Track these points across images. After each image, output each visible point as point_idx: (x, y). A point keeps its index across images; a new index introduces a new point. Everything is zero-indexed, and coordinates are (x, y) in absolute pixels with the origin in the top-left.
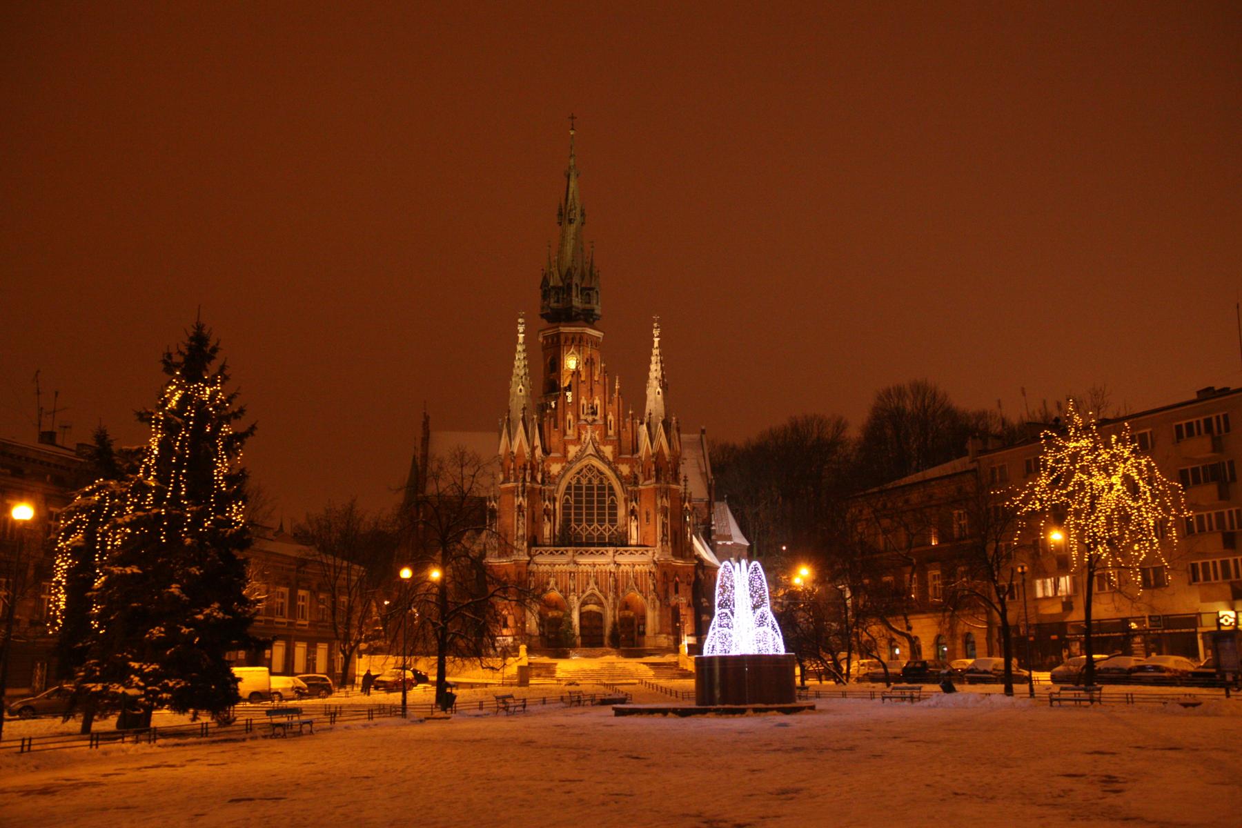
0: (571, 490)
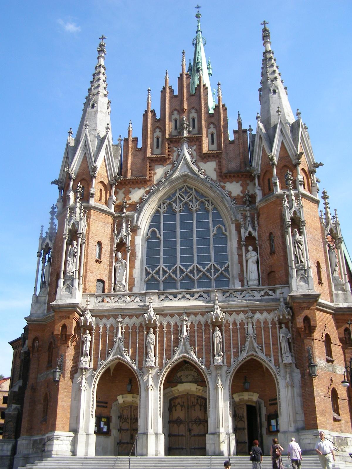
0: (159, 221)
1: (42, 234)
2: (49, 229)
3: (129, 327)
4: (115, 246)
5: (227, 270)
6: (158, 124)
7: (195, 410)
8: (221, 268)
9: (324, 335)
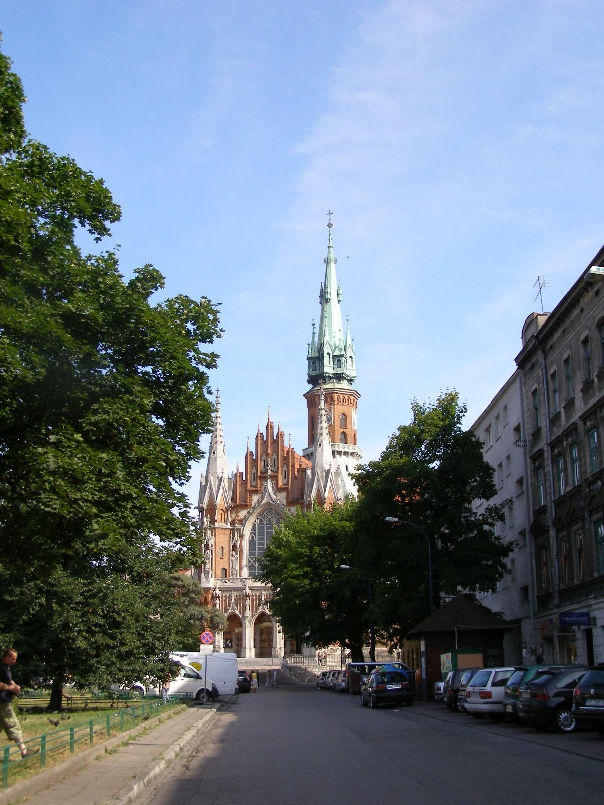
4: (231, 548)
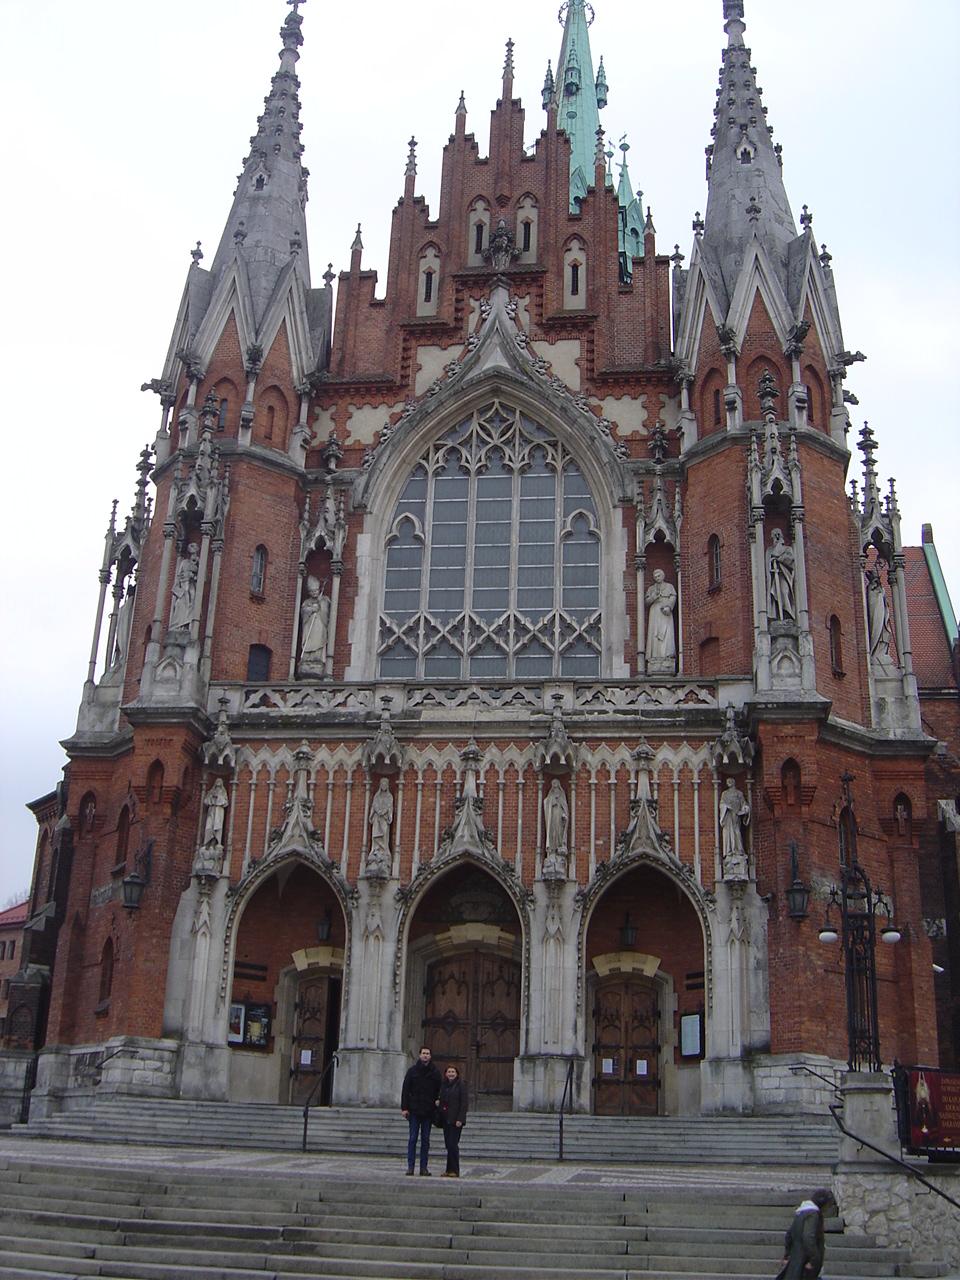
0: (423, 495)
1: (113, 521)
2: (133, 509)
3: (327, 772)
5: (594, 628)
6: (430, 236)
7: (493, 995)
8: (581, 623)
9: (838, 811)
